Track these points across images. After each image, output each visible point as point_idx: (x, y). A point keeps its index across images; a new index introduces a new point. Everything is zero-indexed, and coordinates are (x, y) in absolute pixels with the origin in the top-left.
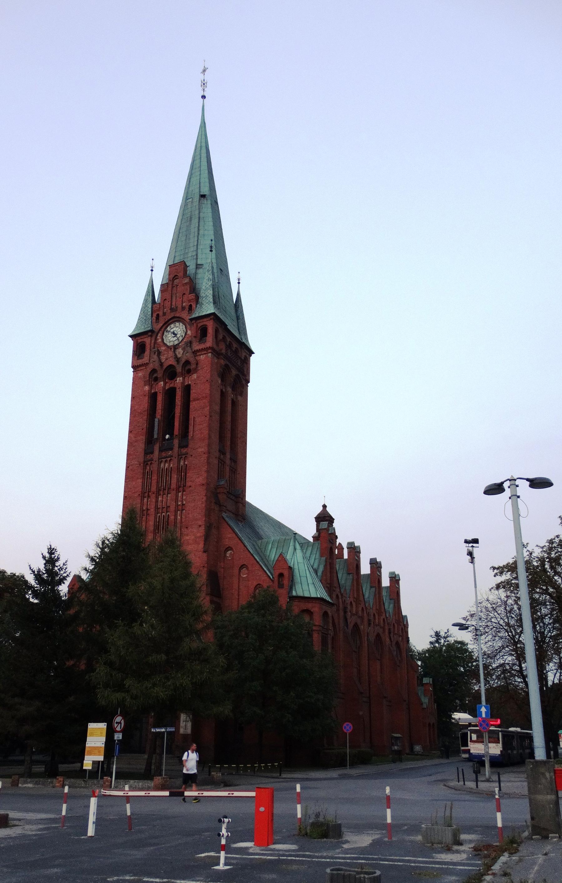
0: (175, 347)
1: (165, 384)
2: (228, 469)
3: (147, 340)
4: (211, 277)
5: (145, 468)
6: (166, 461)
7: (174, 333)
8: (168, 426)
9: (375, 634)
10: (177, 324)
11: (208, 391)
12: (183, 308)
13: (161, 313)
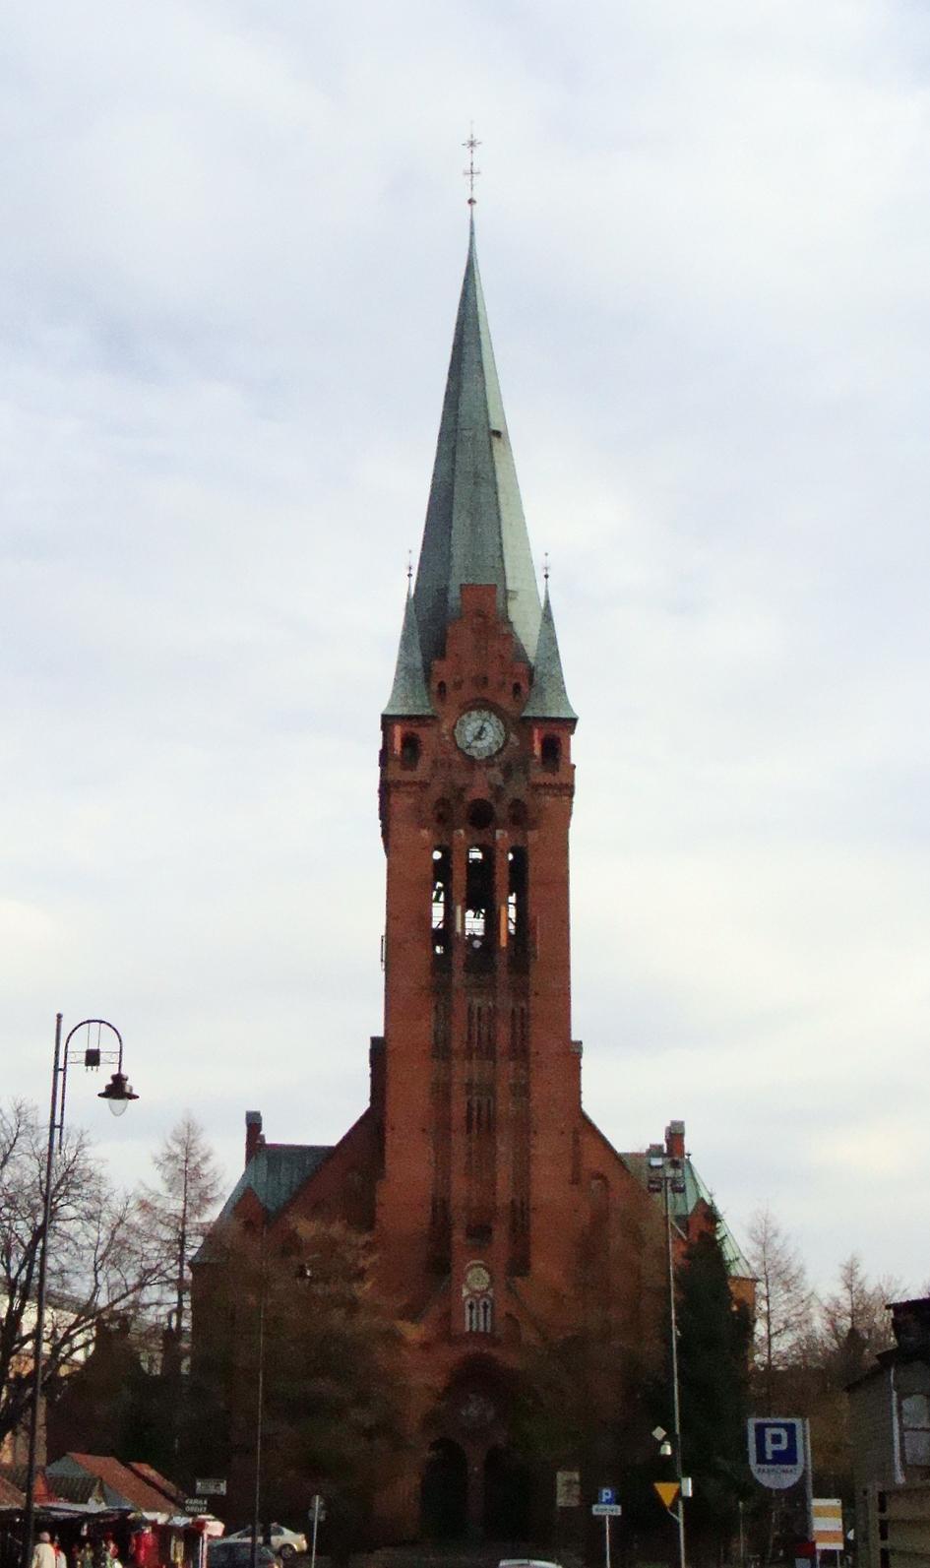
0: (489, 761)
3: (425, 735)
7: (480, 733)
13: (449, 685)
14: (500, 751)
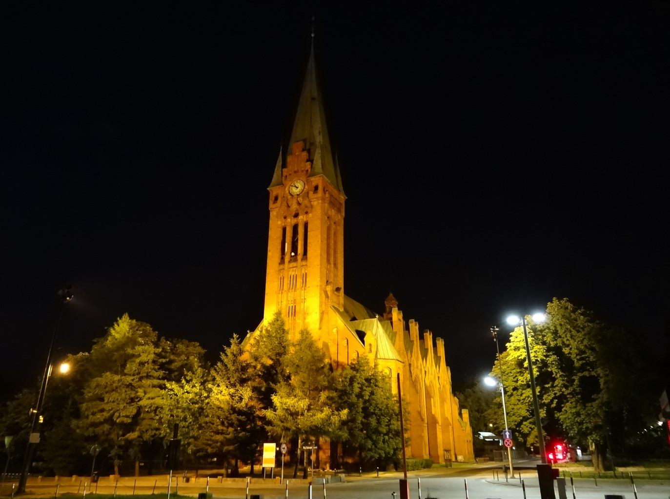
1: (291, 220)
2: (332, 274)
4: (320, 151)
6: (293, 271)
8: (294, 248)
9: (429, 380)
10: (299, 181)
12: (302, 171)
14: (302, 192)
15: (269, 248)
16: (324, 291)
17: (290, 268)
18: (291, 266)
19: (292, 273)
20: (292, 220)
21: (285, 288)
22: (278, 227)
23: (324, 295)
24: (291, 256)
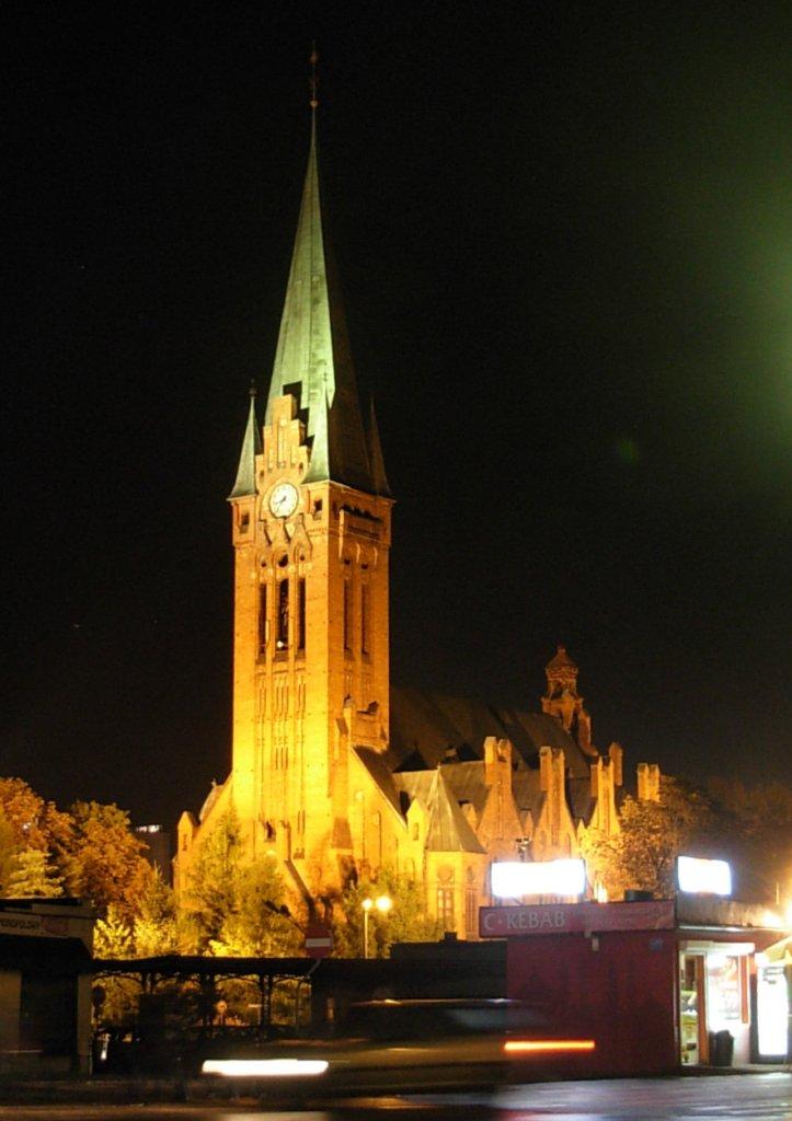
5: (256, 685)
6: (281, 678)
11: (325, 588)
12: (293, 465)
15: (237, 628)
16: (338, 720)
17: (277, 672)
18: (278, 669)
19: (279, 683)
20: (278, 572)
21: (268, 713)
22: (252, 586)
23: (337, 730)
24: (277, 649)
